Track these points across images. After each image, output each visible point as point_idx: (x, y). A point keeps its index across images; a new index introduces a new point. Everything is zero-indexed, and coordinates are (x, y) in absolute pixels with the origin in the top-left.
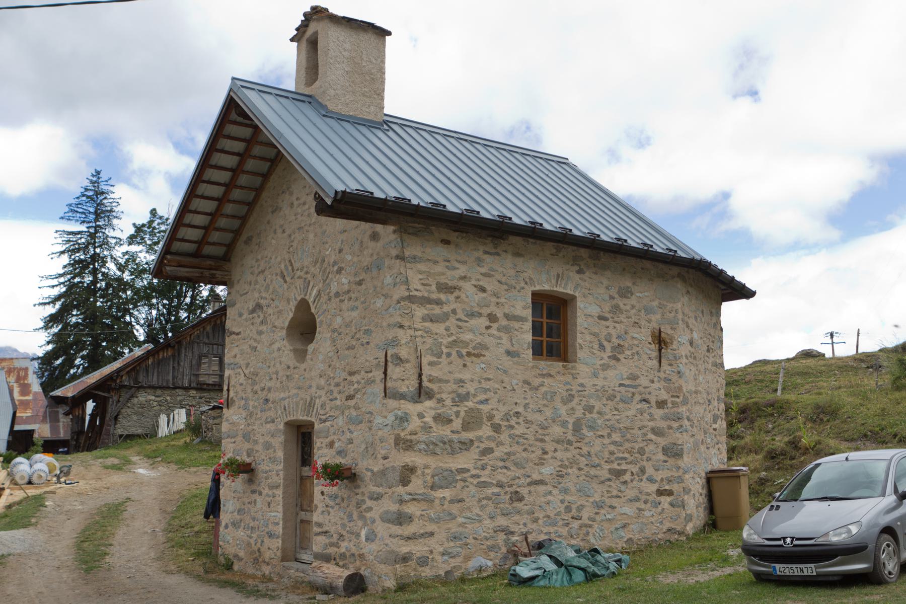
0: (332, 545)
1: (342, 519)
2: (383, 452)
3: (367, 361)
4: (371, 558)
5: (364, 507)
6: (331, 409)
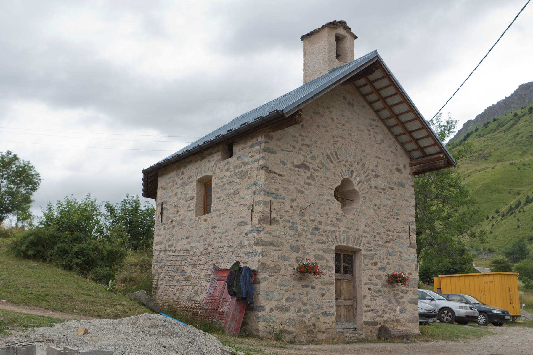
0: (380, 316)
2: (409, 271)
4: (404, 321)
5: (399, 296)
6: (375, 245)
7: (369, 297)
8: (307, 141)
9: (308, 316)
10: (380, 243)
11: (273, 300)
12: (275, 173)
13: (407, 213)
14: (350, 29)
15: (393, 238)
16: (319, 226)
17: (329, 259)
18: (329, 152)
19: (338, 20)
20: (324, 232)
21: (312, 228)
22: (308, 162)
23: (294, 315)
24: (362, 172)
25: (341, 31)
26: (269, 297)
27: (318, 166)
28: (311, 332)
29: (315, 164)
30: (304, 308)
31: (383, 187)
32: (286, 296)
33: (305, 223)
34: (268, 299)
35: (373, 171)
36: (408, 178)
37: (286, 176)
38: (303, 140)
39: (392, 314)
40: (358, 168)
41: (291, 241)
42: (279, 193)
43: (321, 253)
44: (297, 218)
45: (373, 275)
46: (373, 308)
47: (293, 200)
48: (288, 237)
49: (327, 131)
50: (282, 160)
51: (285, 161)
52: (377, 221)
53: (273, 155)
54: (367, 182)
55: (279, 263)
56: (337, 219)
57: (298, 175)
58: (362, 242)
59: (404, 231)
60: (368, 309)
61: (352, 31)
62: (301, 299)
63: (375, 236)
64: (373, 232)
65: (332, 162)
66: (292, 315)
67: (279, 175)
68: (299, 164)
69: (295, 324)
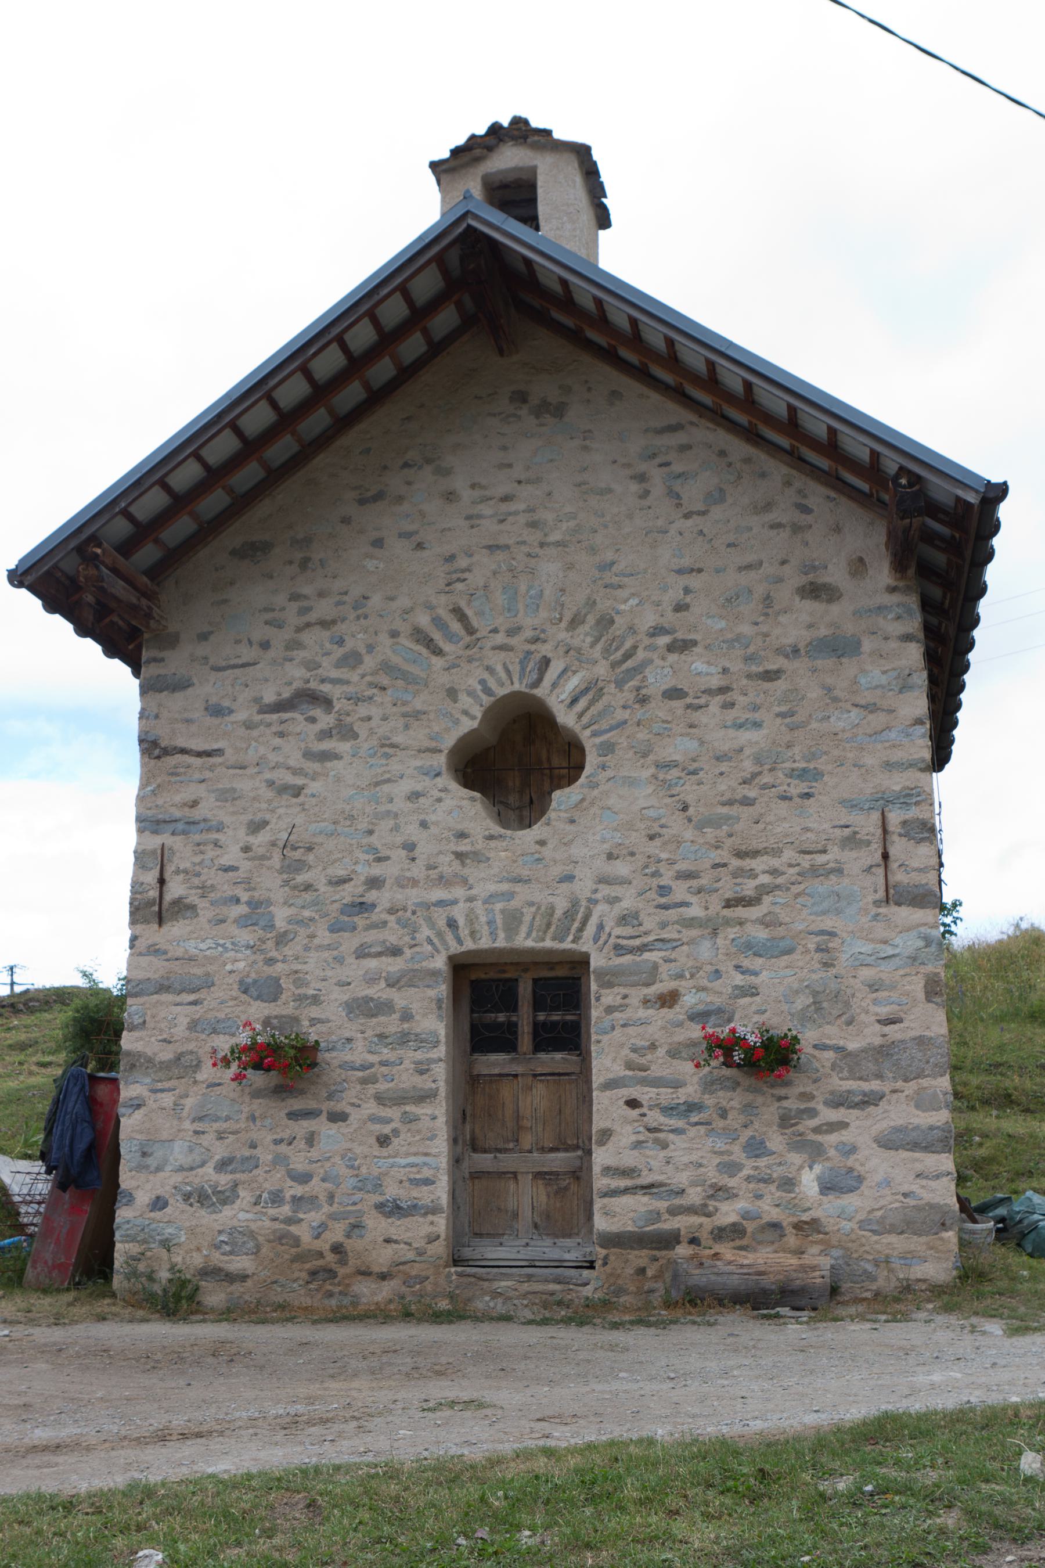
0: (691, 1210)
1: (729, 1153)
3: (807, 829)
7: (626, 1135)
8: (324, 609)
9: (313, 1217)
10: (695, 911)
11: (168, 1168)
12: (183, 751)
13: (869, 761)
14: (548, 133)
15: (779, 880)
16: (372, 896)
17: (415, 1007)
18: (423, 620)
19: (481, 130)
20: (392, 911)
21: (336, 906)
22: (323, 681)
23: (249, 1216)
24: (597, 652)
25: (509, 159)
26: (149, 1161)
27: (371, 685)
28: (321, 1276)
29: (355, 677)
30: (299, 1190)
31: (715, 682)
32: (220, 1151)
33: (308, 896)
34: (147, 1167)
35: (658, 631)
36: (880, 609)
37: (229, 752)
38: (304, 611)
39: (768, 1199)
40: (576, 642)
41: (241, 965)
42: (197, 814)
43: (378, 991)
44: (270, 883)
45: (653, 1047)
46: (646, 1179)
47: (256, 827)
48: (232, 954)
49: (420, 546)
50: (214, 700)
51: (226, 703)
52: (676, 825)
53: (179, 695)
54: (620, 684)
55: (191, 1046)
56: (460, 856)
57: (281, 735)
58: (593, 921)
59: (852, 841)
60: (623, 1183)
61: (557, 135)
62: (279, 1160)
63: (664, 890)
64: (656, 874)
65: (438, 652)
66: (242, 1216)
67: (199, 754)
68: (286, 695)
69: (258, 1247)
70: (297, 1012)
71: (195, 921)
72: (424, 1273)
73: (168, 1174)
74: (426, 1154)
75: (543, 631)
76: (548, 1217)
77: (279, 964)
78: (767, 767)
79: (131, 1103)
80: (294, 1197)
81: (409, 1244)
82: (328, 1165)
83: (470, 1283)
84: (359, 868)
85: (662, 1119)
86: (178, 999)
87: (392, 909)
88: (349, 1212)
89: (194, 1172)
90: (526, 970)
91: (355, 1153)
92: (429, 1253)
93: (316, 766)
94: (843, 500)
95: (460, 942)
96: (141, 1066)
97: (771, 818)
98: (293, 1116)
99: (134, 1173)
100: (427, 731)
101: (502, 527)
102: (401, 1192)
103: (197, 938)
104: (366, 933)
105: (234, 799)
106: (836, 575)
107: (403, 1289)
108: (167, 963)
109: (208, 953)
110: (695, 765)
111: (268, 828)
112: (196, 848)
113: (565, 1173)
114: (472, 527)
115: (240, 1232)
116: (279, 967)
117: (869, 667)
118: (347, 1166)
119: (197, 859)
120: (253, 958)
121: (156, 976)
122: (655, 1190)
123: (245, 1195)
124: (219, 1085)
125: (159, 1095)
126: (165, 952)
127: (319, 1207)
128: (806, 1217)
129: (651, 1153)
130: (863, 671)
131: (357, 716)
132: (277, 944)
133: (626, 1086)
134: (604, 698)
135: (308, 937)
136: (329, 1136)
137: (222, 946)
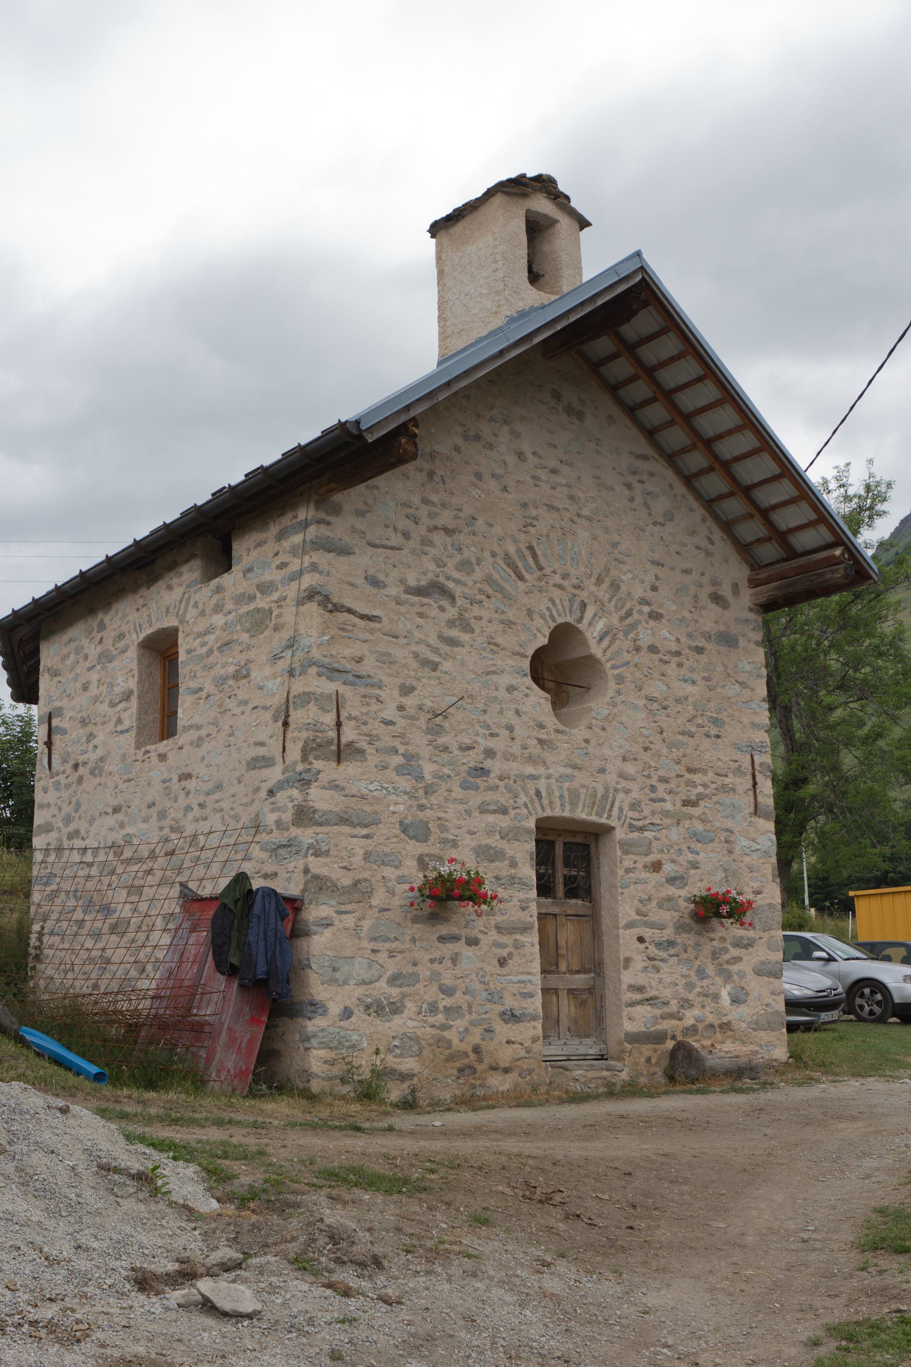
0: (672, 1016)
1: (688, 976)
2: (756, 885)
3: (719, 759)
4: (744, 1025)
5: (726, 957)
6: (653, 813)
7: (639, 962)
8: (445, 518)
9: (459, 1024)
10: (668, 806)
11: (352, 982)
12: (350, 611)
13: (745, 720)
14: (567, 198)
15: (708, 792)
16: (488, 764)
17: (519, 856)
18: (512, 549)
19: (530, 174)
20: (501, 778)
21: (465, 768)
22: (448, 578)
23: (415, 1023)
24: (611, 607)
25: (542, 205)
26: (338, 975)
27: (480, 590)
28: (467, 1072)
29: (470, 583)
30: (448, 1002)
31: (674, 647)
32: (392, 968)
33: (445, 756)
34: (336, 981)
35: (643, 601)
36: (746, 621)
37: (385, 620)
38: (432, 515)
39: (708, 1009)
40: (601, 595)
41: (401, 808)
42: (362, 669)
43: (494, 841)
44: (419, 742)
45: (650, 899)
46: (652, 993)
47: (406, 690)
48: (393, 797)
49: (505, 489)
50: (371, 571)
51: (381, 577)
52: (658, 746)
53: (344, 559)
54: (626, 634)
55: (366, 875)
56: (541, 741)
57: (421, 615)
58: (617, 805)
59: (738, 771)
60: (639, 997)
61: (573, 204)
62: (435, 976)
63: (653, 788)
64: (649, 776)
65: (521, 578)
66: (410, 1023)
67: (363, 617)
68: (424, 583)
69: (421, 1050)
70: (442, 853)
71: (364, 764)
72: (531, 1067)
73: (353, 987)
74: (529, 973)
75: (582, 581)
76: (576, 1023)
77: (428, 810)
78: (700, 713)
79: (322, 922)
80: (445, 1007)
81: (521, 1044)
82: (467, 981)
83: (559, 1074)
84: (479, 739)
85: (656, 951)
86: (354, 831)
87: (501, 776)
88: (483, 1019)
89: (372, 986)
90: (559, 835)
91: (485, 972)
92: (534, 1051)
93: (447, 648)
94: (729, 542)
95: (543, 809)
96: (327, 889)
97: (702, 748)
98: (442, 939)
99: (326, 985)
100: (517, 638)
101: (553, 492)
102: (515, 1003)
103: (367, 780)
104: (485, 794)
105: (391, 663)
106: (726, 591)
107: (520, 1080)
108: (343, 799)
109: (375, 793)
110: (666, 703)
111: (416, 693)
112: (363, 699)
113: (585, 990)
114: (536, 486)
115: (409, 1037)
116: (429, 813)
117: (742, 658)
118: (481, 982)
119: (365, 710)
120: (410, 802)
121: (337, 809)
122: (652, 1002)
123: (411, 1007)
124: (388, 910)
125: (343, 917)
126: (343, 789)
127: (463, 1016)
128: (725, 1020)
129: (651, 975)
130: (740, 660)
131: (473, 614)
132: (426, 793)
133: (636, 927)
134: (617, 641)
135: (447, 791)
136: (468, 957)
137: (386, 789)
